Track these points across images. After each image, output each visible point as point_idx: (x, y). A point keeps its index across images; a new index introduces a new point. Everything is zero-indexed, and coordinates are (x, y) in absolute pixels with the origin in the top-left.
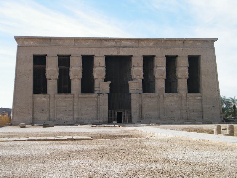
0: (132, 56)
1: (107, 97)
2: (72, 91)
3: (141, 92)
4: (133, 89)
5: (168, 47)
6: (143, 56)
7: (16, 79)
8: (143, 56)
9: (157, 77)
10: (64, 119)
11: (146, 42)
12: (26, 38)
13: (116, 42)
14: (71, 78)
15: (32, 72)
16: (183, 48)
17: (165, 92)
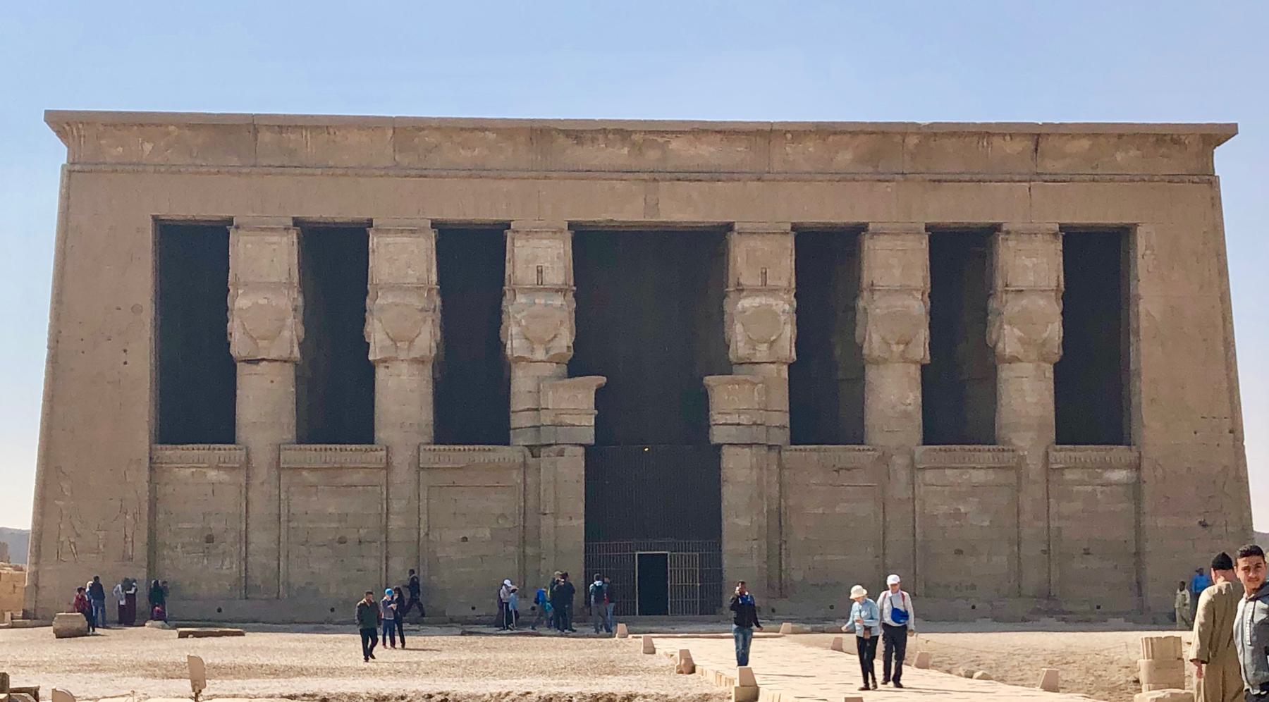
0: (729, 227)
3: (783, 437)
4: (730, 419)
5: (944, 177)
6: (795, 227)
8: (795, 227)
9: (876, 353)
10: (333, 590)
11: (811, 146)
13: (638, 148)
14: (371, 358)
16: (1030, 181)
17: (918, 437)
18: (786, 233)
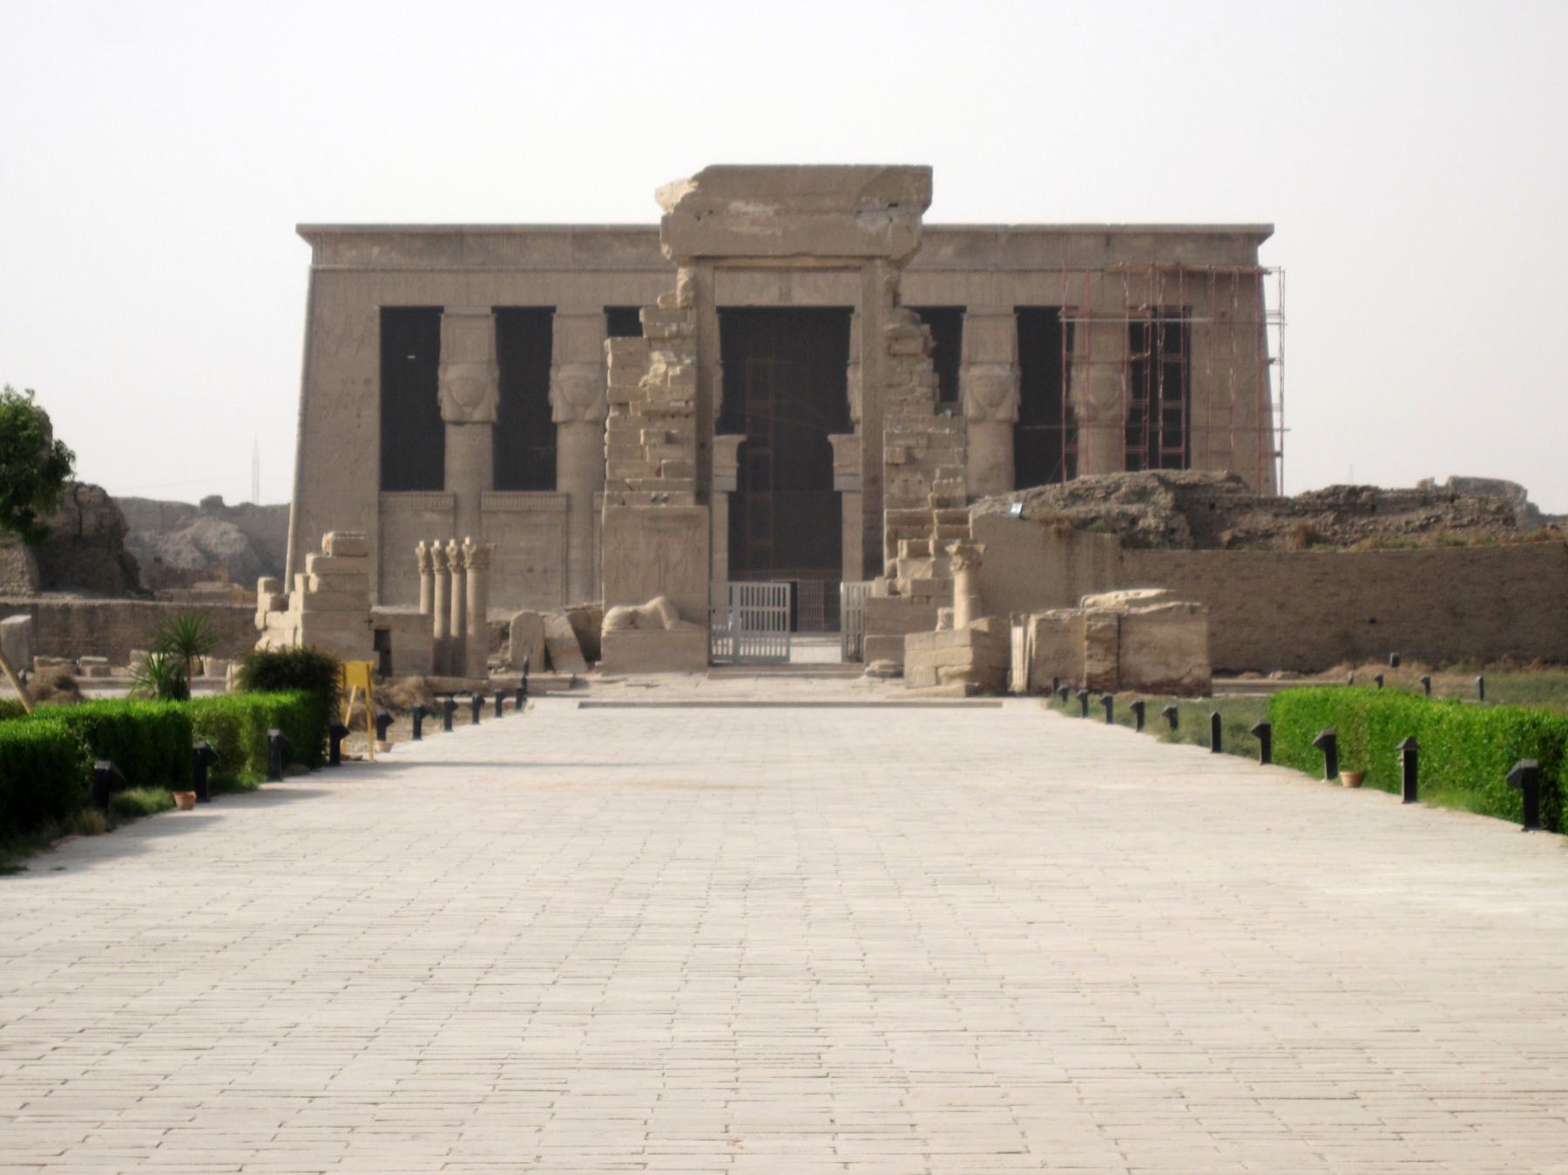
2: (565, 482)
4: (849, 470)
15: (376, 388)
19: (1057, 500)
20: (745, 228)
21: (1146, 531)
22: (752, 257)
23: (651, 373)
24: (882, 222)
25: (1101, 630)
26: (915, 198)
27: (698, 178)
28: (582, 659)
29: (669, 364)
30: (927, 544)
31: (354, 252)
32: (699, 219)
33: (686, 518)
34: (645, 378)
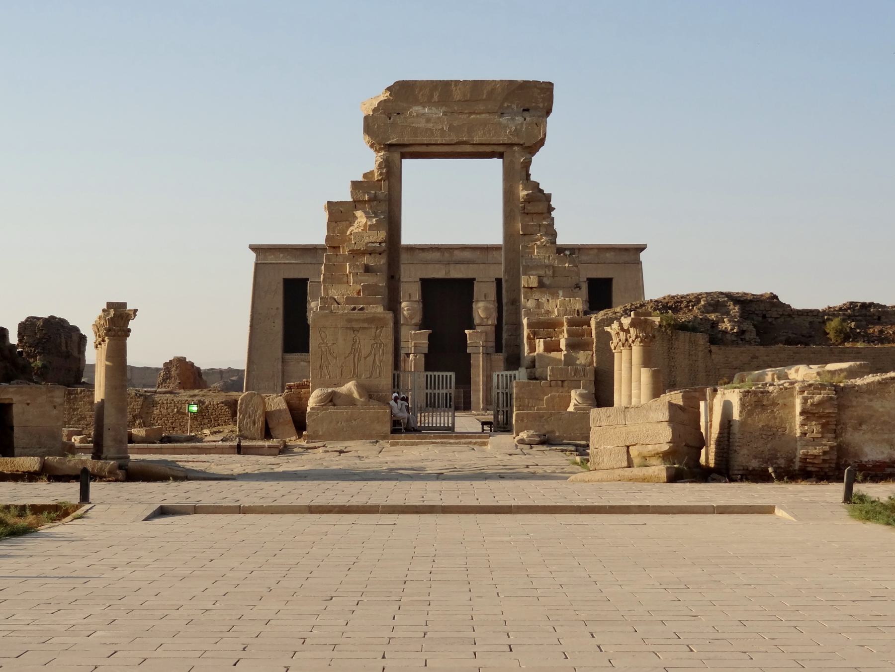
0: (474, 279)
1: (424, 359)
3: (492, 350)
7: (251, 326)
12: (271, 249)
15: (281, 311)
18: (493, 282)
19: (655, 310)
20: (422, 124)
21: (725, 332)
22: (427, 145)
23: (356, 224)
24: (519, 119)
25: (820, 403)
26: (541, 105)
27: (389, 89)
28: (294, 428)
29: (367, 217)
30: (559, 341)
31: (272, 256)
32: (390, 119)
33: (372, 320)
34: (351, 228)
